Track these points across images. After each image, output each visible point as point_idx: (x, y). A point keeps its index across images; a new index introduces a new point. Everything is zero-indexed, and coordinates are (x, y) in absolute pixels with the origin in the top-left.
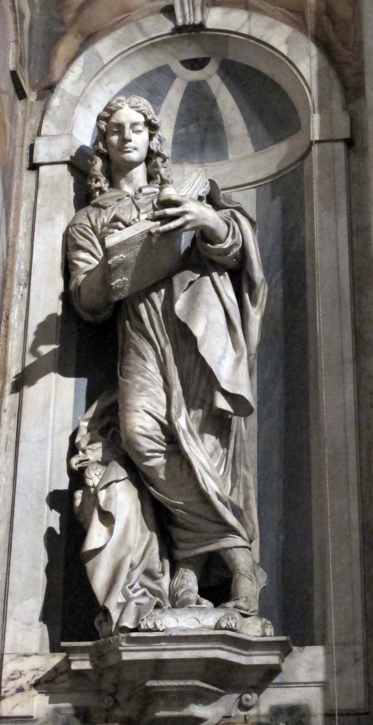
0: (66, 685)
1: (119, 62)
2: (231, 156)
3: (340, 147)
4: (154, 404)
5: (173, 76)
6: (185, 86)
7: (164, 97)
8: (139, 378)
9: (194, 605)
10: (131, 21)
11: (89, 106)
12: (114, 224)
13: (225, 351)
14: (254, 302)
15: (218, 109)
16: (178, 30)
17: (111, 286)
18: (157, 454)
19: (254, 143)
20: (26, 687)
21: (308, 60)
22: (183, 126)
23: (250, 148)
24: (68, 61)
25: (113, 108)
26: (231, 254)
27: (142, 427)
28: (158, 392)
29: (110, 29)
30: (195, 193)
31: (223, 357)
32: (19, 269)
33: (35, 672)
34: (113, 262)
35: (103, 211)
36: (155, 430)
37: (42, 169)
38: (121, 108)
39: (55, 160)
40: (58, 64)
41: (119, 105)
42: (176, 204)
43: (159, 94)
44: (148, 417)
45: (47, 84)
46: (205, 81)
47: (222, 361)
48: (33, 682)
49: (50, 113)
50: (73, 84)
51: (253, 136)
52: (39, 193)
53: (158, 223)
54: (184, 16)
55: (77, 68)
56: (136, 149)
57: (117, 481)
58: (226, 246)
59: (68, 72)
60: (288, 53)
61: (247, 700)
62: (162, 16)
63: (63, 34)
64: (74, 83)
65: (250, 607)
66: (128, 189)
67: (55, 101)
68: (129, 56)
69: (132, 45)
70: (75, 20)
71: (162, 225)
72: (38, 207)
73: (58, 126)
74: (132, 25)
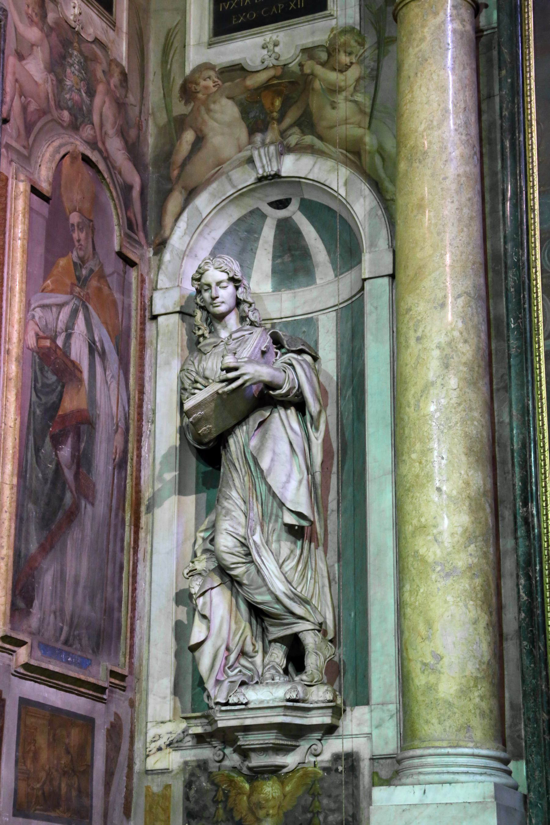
0: (190, 744)
1: (216, 214)
2: (318, 281)
3: (386, 280)
4: (235, 526)
5: (264, 216)
6: (275, 223)
7: (260, 234)
8: (226, 504)
9: (270, 681)
10: (222, 174)
11: (196, 256)
12: (195, 385)
13: (289, 476)
14: (317, 429)
15: (304, 240)
16: (260, 179)
17: (199, 434)
18: (239, 565)
19: (334, 270)
20: (163, 746)
21: (362, 200)
22: (280, 257)
23: (331, 275)
24: (175, 217)
25: (201, 271)
26: (291, 395)
27: (225, 546)
28: (239, 515)
29: (208, 182)
30: (257, 349)
31: (288, 481)
32: (147, 408)
33: (169, 735)
34: (193, 419)
35: (204, 357)
36: (236, 547)
37: (160, 319)
38: (207, 270)
39: (168, 311)
40: (168, 220)
41: (206, 267)
42: (236, 369)
43: (255, 232)
44: (230, 538)
45: (160, 240)
46: (290, 217)
47: (287, 485)
48: (168, 743)
49: (163, 267)
50: (180, 239)
51: (333, 262)
52: (159, 340)
53: (224, 384)
54: (263, 167)
55: (182, 224)
56: (223, 302)
57: (212, 588)
58: (283, 391)
59: (176, 228)
60: (346, 195)
61: (315, 750)
62: (246, 166)
63: (170, 191)
64: (181, 238)
65: (313, 679)
66: (224, 334)
67: (167, 256)
68: (223, 208)
69: (224, 198)
70: (179, 176)
71: (227, 385)
72: (159, 353)
73: (170, 279)
74: (224, 177)
